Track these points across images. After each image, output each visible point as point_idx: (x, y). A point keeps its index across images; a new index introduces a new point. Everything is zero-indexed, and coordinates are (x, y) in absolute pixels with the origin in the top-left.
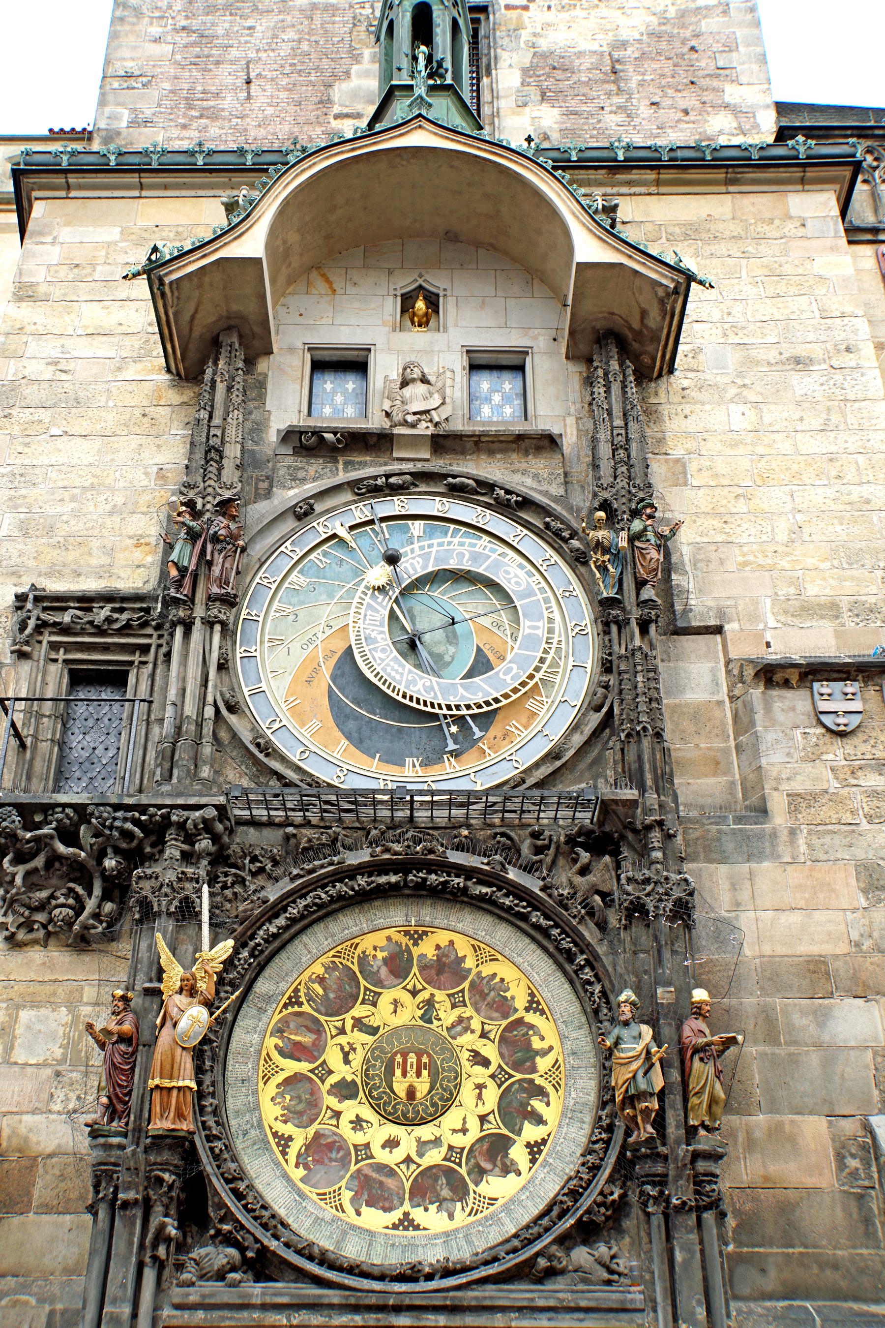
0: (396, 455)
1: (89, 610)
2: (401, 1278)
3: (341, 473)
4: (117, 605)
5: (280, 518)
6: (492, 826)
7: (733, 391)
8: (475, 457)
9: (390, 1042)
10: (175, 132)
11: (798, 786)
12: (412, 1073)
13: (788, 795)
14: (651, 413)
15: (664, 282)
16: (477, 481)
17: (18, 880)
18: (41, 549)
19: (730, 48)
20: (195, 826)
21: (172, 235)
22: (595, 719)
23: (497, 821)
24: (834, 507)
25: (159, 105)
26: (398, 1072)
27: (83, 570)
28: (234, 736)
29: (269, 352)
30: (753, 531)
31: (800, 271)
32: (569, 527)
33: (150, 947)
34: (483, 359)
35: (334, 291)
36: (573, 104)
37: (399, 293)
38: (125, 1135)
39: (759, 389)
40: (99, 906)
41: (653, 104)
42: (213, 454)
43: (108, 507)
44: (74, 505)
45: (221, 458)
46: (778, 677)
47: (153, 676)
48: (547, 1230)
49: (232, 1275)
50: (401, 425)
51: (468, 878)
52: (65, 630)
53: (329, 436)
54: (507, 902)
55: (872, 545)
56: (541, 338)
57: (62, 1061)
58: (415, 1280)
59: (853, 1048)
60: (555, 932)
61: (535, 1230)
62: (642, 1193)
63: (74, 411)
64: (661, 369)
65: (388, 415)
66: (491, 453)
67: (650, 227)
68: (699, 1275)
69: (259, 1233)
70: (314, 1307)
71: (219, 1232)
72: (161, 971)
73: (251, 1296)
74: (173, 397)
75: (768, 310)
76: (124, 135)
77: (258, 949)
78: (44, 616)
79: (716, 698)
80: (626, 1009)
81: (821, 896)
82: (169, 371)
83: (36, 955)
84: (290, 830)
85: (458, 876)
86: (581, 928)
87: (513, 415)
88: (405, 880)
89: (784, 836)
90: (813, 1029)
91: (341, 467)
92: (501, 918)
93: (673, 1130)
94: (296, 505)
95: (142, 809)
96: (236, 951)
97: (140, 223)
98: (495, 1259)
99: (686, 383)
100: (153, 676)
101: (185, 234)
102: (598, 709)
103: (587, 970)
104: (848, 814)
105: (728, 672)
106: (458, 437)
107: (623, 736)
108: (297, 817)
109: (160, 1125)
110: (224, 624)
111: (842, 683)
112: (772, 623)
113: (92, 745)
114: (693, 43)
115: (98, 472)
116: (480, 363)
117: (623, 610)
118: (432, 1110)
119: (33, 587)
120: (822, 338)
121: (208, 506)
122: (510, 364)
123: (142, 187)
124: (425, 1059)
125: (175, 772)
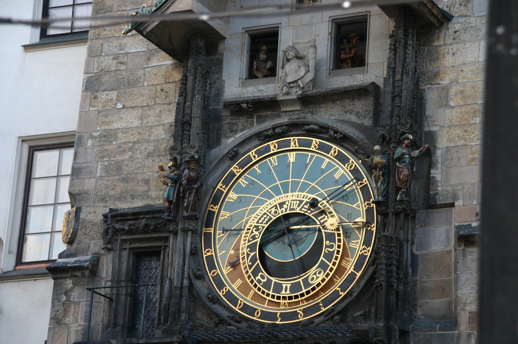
0: (282, 110)
3: (255, 125)
4: (150, 216)
5: (222, 160)
13: (469, 313)
43: (146, 153)
44: (130, 154)
53: (244, 105)
63: (127, 90)
66: (334, 101)
78: (118, 226)
79: (447, 249)
94: (228, 153)
99: (457, 27)
115: (141, 132)
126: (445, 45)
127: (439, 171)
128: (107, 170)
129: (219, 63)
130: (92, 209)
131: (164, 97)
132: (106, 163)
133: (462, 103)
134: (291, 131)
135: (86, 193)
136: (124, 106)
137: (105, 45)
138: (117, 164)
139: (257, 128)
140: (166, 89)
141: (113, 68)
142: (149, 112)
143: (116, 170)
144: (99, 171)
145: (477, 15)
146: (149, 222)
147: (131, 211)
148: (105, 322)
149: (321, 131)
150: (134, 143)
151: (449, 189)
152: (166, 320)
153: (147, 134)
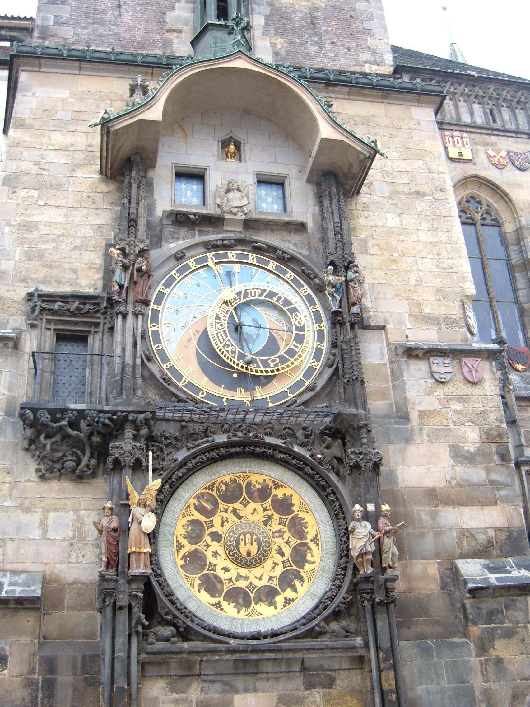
0: (225, 228)
1: (67, 302)
2: (253, 638)
3: (197, 236)
5: (168, 259)
6: (282, 424)
8: (264, 232)
10: (80, 31)
11: (424, 407)
12: (249, 543)
15: (364, 152)
16: (267, 245)
17: (48, 447)
19: (370, 18)
20: (141, 422)
21: (98, 97)
24: (436, 270)
25: (71, 15)
26: (242, 543)
28: (152, 375)
29: (153, 166)
30: (399, 279)
31: (418, 147)
33: (120, 483)
34: (264, 178)
35: (186, 136)
36: (292, 38)
37: (220, 139)
38: (117, 575)
40: (89, 461)
41: (332, 43)
42: (132, 223)
43: (72, 246)
44: (54, 244)
45: (137, 225)
46: (414, 353)
47: (102, 340)
48: (318, 615)
49: (173, 639)
50: (227, 213)
53: (192, 217)
54: (293, 462)
55: (454, 290)
56: (293, 170)
57: (73, 538)
58: (258, 639)
59: (447, 530)
60: (317, 477)
61: (313, 615)
62: (362, 597)
63: (50, 192)
64: (354, 192)
65: (219, 206)
66: (273, 231)
67: (345, 116)
72: (128, 495)
73: (183, 648)
74: (104, 188)
75: (404, 166)
76: (51, 30)
78: (45, 305)
82: (101, 172)
83: (55, 485)
84: (183, 423)
85: (269, 449)
86: (330, 475)
87: (278, 209)
89: (417, 431)
90: (430, 522)
91: (197, 233)
95: (114, 413)
96: (163, 486)
97: (80, 89)
98: (296, 629)
99: (365, 200)
100: (102, 340)
102: (331, 366)
103: (332, 495)
104: (445, 421)
105: (389, 349)
106: (256, 221)
107: (346, 381)
108: (187, 417)
110: (143, 315)
112: (409, 326)
114: (352, 14)
117: (342, 317)
118: (259, 561)
119: (37, 289)
120: (430, 183)
121: (132, 251)
122: (275, 182)
124: (255, 537)
127: (369, 300)
128: (28, 256)
129: (150, 186)
130: (11, 288)
132: (26, 249)
134: (236, 246)
135: (3, 272)
136: (46, 204)
137: (25, 154)
140: (93, 197)
142: (75, 213)
149: (269, 251)
150: (59, 236)
151: (380, 315)
152: (121, 394)
153: (73, 230)
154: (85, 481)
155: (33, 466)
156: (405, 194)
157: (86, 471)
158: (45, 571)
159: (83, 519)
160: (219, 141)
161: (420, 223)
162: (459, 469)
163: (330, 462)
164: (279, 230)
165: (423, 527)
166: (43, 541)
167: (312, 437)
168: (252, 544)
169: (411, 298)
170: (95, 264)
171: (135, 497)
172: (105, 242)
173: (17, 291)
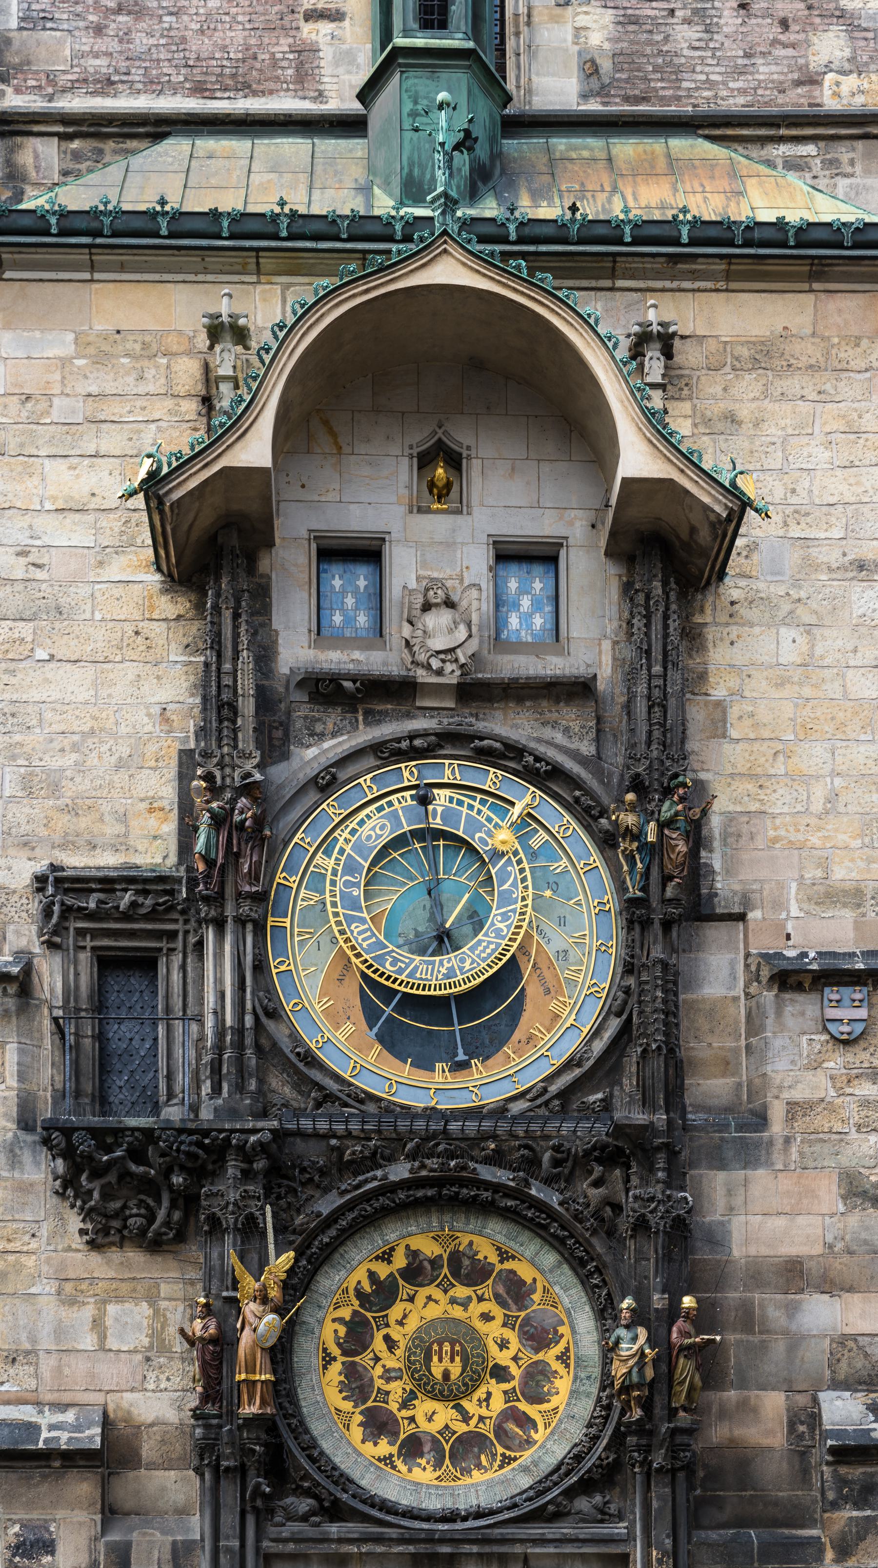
2: (444, 1519)
4: (140, 887)
6: (517, 1137)
7: (786, 607)
9: (428, 1333)
11: (798, 1094)
14: (693, 637)
16: (505, 744)
18: (50, 813)
21: (138, 347)
22: (614, 1024)
23: (521, 1134)
26: (435, 1359)
27: (99, 841)
30: (788, 799)
32: (599, 803)
39: (814, 606)
40: (169, 1215)
43: (113, 760)
44: (74, 756)
46: (792, 980)
48: (556, 1484)
49: (313, 1519)
51: (495, 1192)
52: (92, 916)
57: (150, 1348)
60: (570, 1242)
62: (631, 1458)
63: (57, 625)
64: (710, 578)
68: (669, 1518)
69: (332, 1488)
70: (378, 1540)
71: (299, 1487)
73: (328, 1533)
77: (315, 1257)
78: (69, 901)
80: (625, 1314)
81: (805, 1201)
82: (159, 569)
83: (115, 1255)
84: (333, 1142)
85: (486, 1190)
88: (440, 1193)
89: (779, 1144)
92: (524, 1226)
93: (658, 1411)
96: (297, 1260)
98: (515, 1506)
99: (736, 594)
101: (155, 347)
102: (619, 1014)
108: (340, 1128)
109: (250, 1409)
111: (851, 989)
112: (795, 912)
113: (128, 1035)
116: (508, 554)
119: (53, 868)
123: (92, 268)
125: (225, 1087)
126: (717, 624)
128: (28, 786)
131: (143, 648)
132: (22, 770)
133: (752, 736)
136: (52, 656)
138: (48, 775)
139: (366, 735)
140: (145, 632)
141: (19, 574)
142: (111, 676)
143: (49, 786)
144: (7, 784)
145: (769, 578)
146: (141, 900)
147: (100, 874)
148: (59, 1086)
153: (112, 720)
154: (165, 1247)
155: (75, 1222)
156: (830, 569)
157: (166, 1234)
158: (105, 1406)
159: (164, 1316)
160: (411, 457)
161: (855, 651)
162: (854, 1220)
163: (597, 1214)
164: (534, 698)
165: (768, 1332)
166: (101, 1355)
167: (569, 1164)
168: (452, 1360)
169: (809, 844)
170: (162, 798)
171: (249, 1284)
172: (177, 746)
173: (14, 869)
